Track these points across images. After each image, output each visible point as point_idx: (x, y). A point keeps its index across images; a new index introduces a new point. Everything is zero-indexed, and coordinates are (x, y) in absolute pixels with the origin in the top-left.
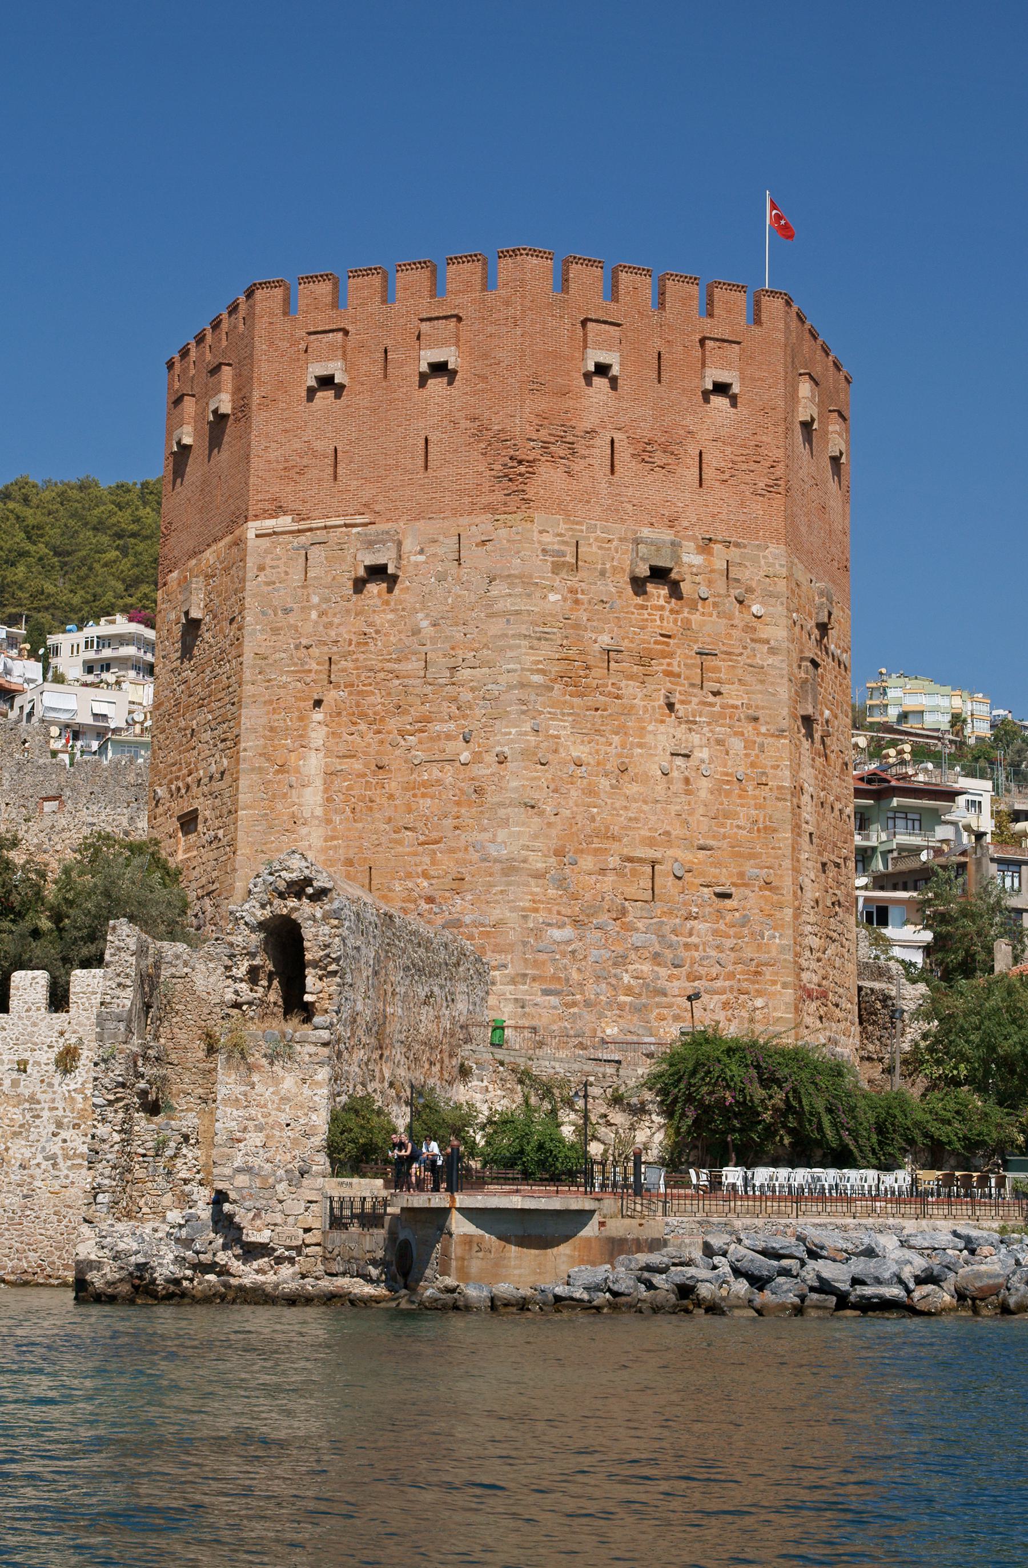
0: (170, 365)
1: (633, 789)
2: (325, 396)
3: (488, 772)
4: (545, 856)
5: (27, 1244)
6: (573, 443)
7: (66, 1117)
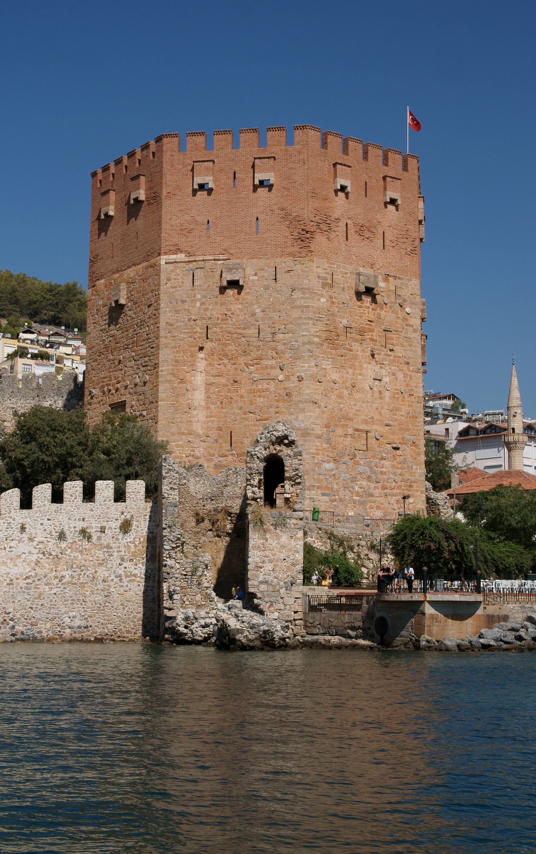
0: (94, 175)
1: (358, 396)
2: (203, 195)
3: (293, 385)
4: (322, 428)
5: (108, 620)
6: (330, 224)
7: (126, 555)
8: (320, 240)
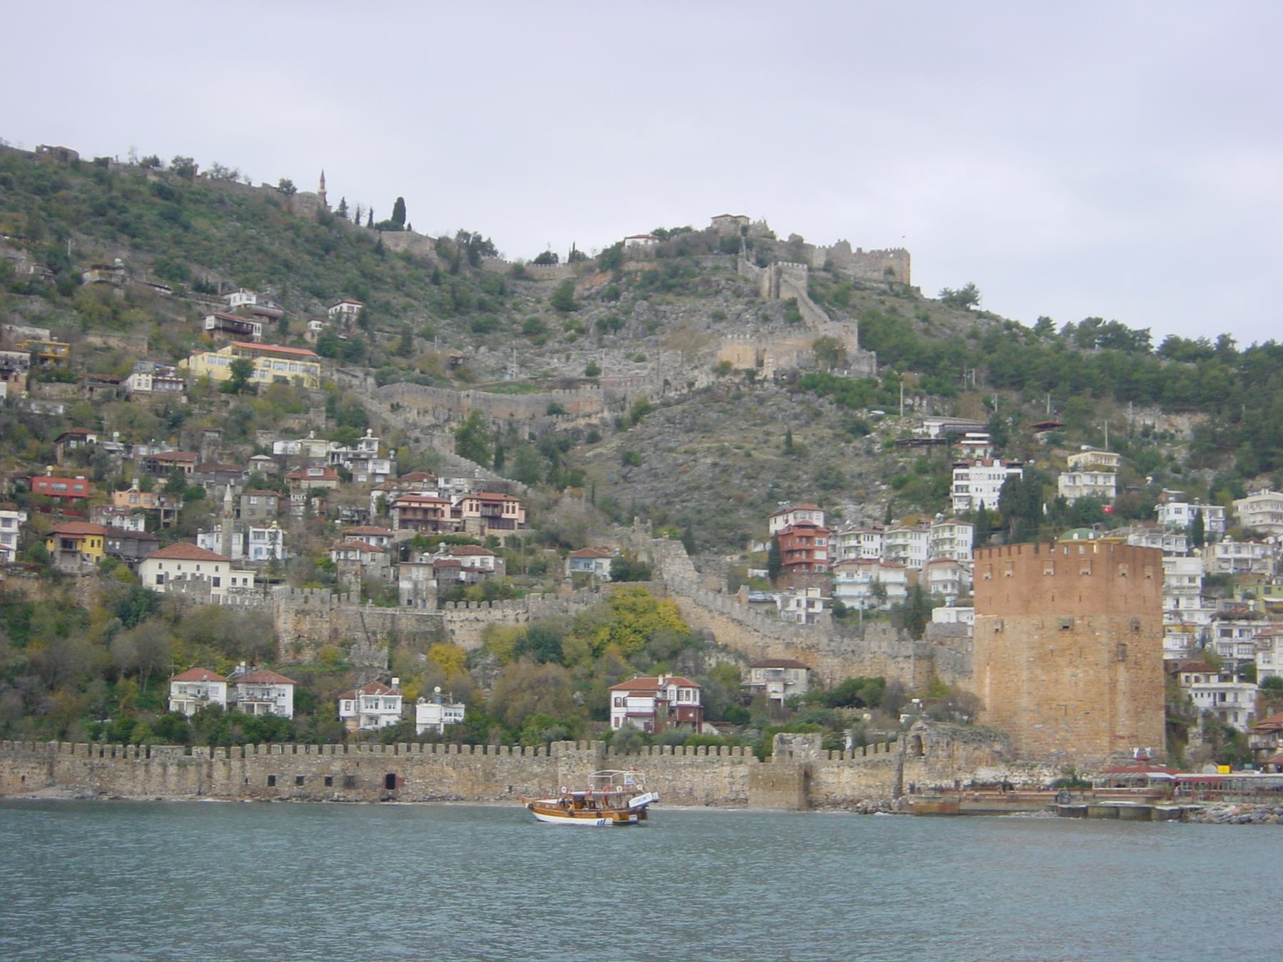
1: (1060, 686)
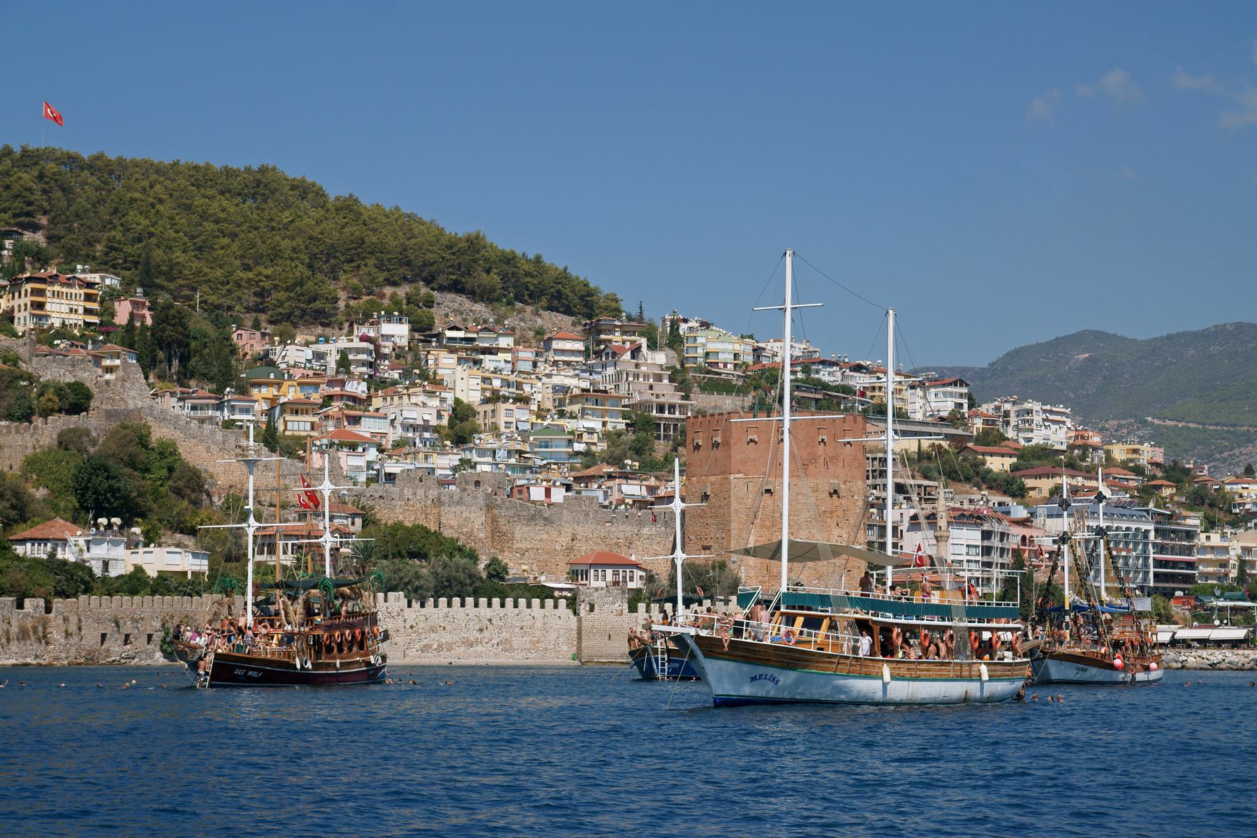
2: (752, 444)
8: (811, 468)
